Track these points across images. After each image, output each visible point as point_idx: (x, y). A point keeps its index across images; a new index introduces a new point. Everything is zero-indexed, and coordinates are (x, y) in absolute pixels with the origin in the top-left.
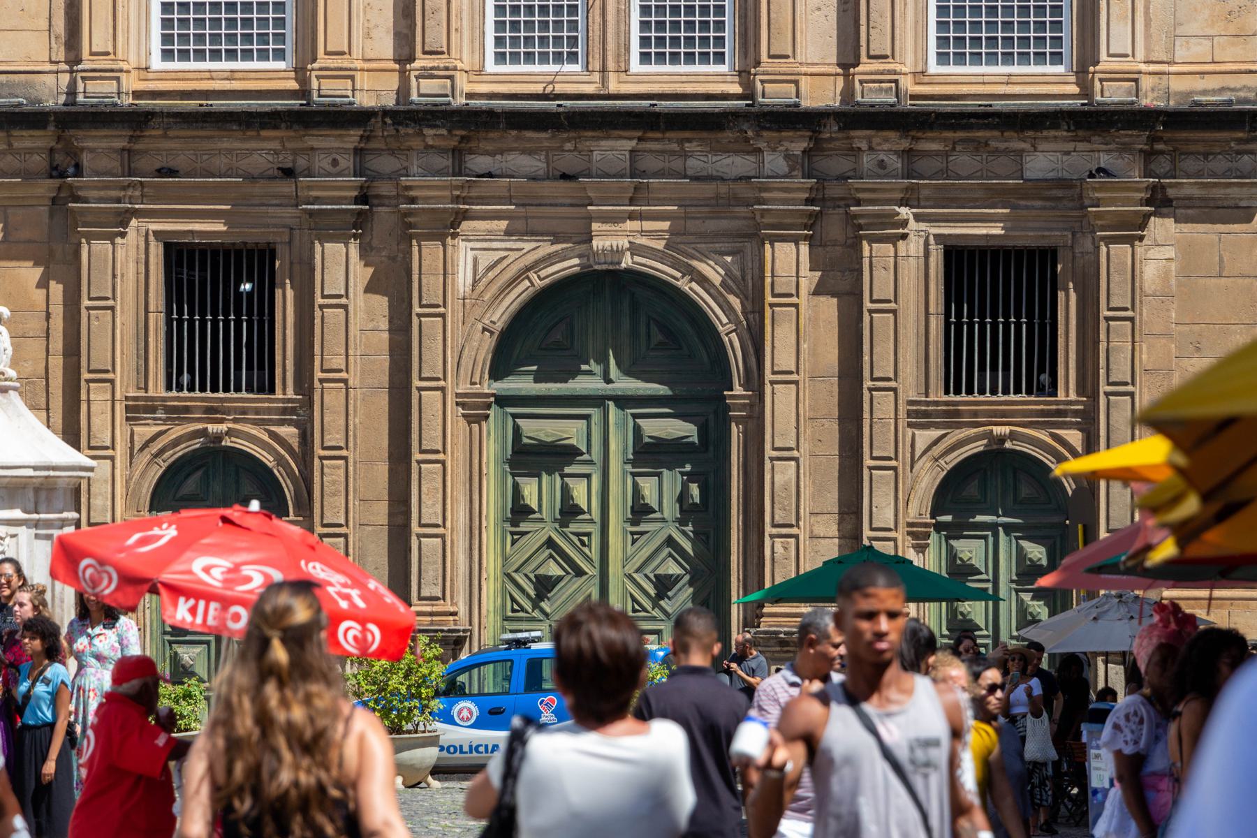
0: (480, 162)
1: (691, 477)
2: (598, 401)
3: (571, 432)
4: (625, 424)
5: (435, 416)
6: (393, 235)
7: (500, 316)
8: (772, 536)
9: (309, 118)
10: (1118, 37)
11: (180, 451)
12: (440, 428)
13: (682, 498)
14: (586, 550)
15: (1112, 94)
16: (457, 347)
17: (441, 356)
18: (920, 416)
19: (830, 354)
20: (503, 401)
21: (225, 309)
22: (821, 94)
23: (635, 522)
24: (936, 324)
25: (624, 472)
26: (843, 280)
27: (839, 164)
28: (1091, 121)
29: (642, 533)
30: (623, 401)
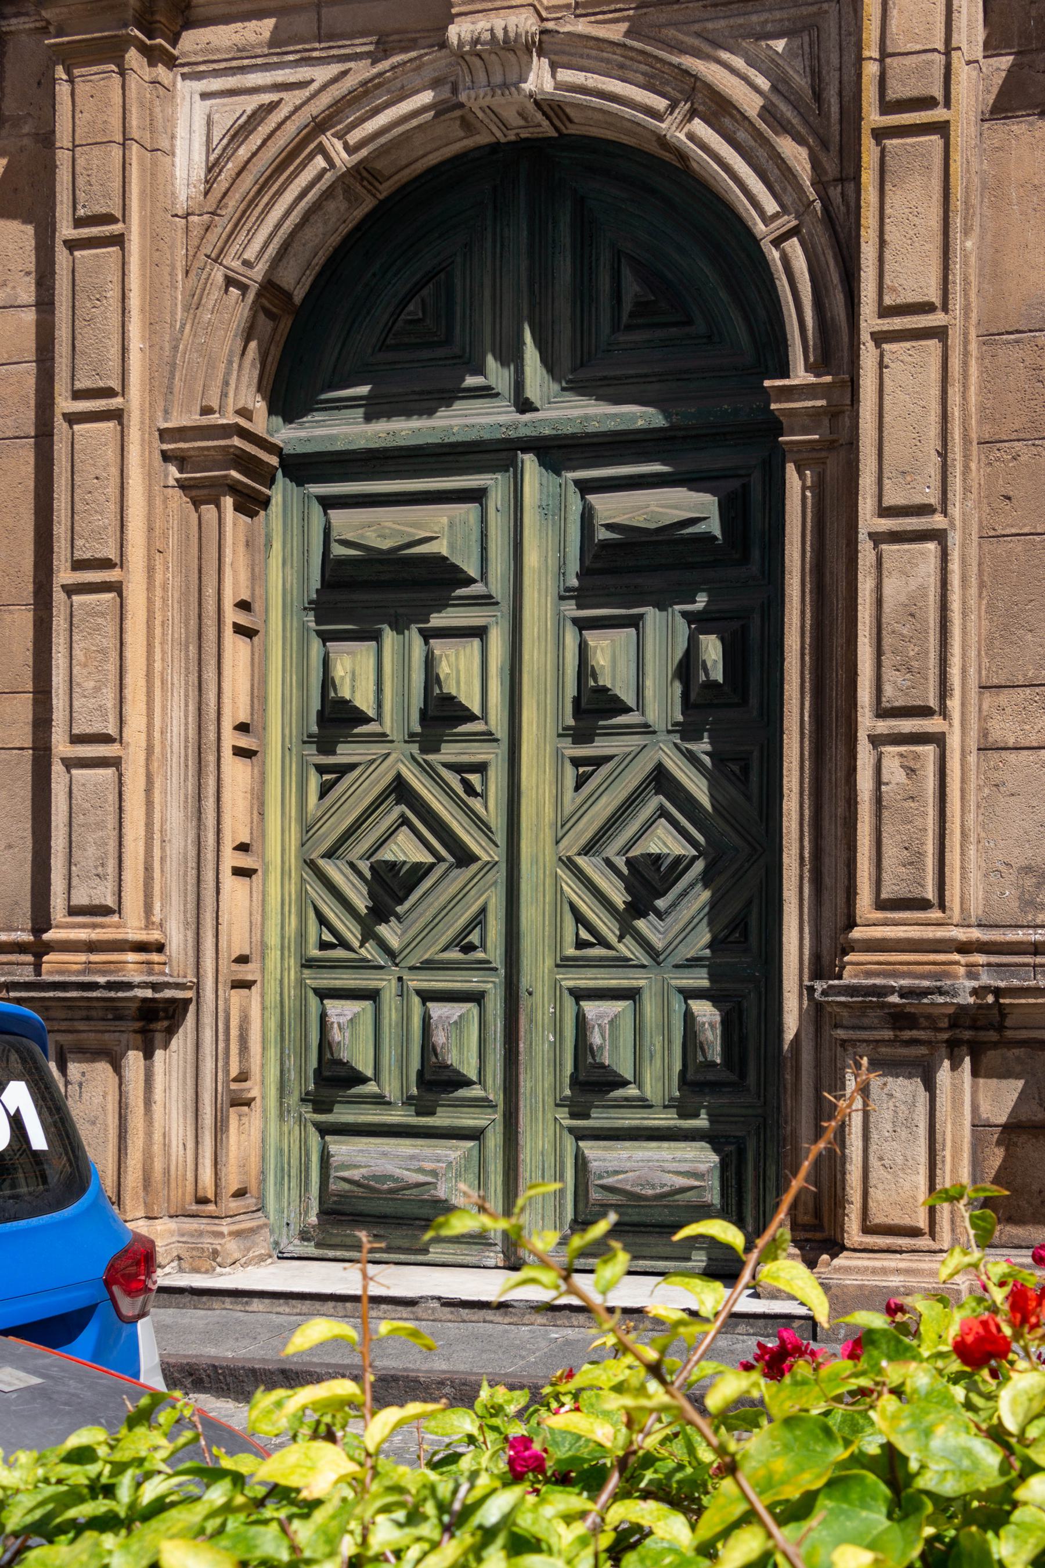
1: (700, 622)
2: (498, 453)
3: (440, 530)
4: (563, 507)
8: (876, 741)
12: (113, 507)
13: (687, 668)
14: (476, 804)
17: (116, 337)
20: (302, 468)
23: (581, 735)
25: (560, 621)
29: (598, 762)
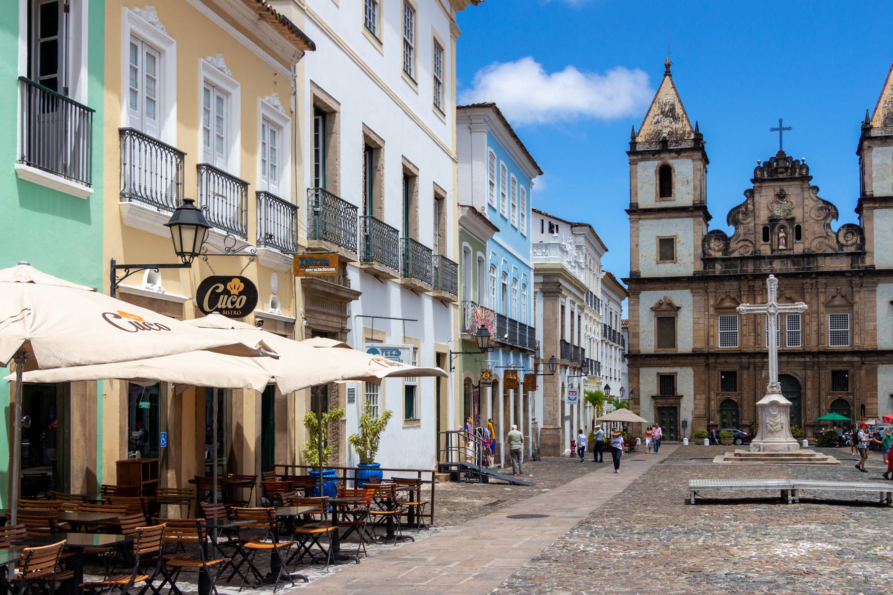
10: (857, 341)
15: (856, 349)
18: (829, 394)
21: (730, 380)
22: (815, 350)
28: (853, 353)
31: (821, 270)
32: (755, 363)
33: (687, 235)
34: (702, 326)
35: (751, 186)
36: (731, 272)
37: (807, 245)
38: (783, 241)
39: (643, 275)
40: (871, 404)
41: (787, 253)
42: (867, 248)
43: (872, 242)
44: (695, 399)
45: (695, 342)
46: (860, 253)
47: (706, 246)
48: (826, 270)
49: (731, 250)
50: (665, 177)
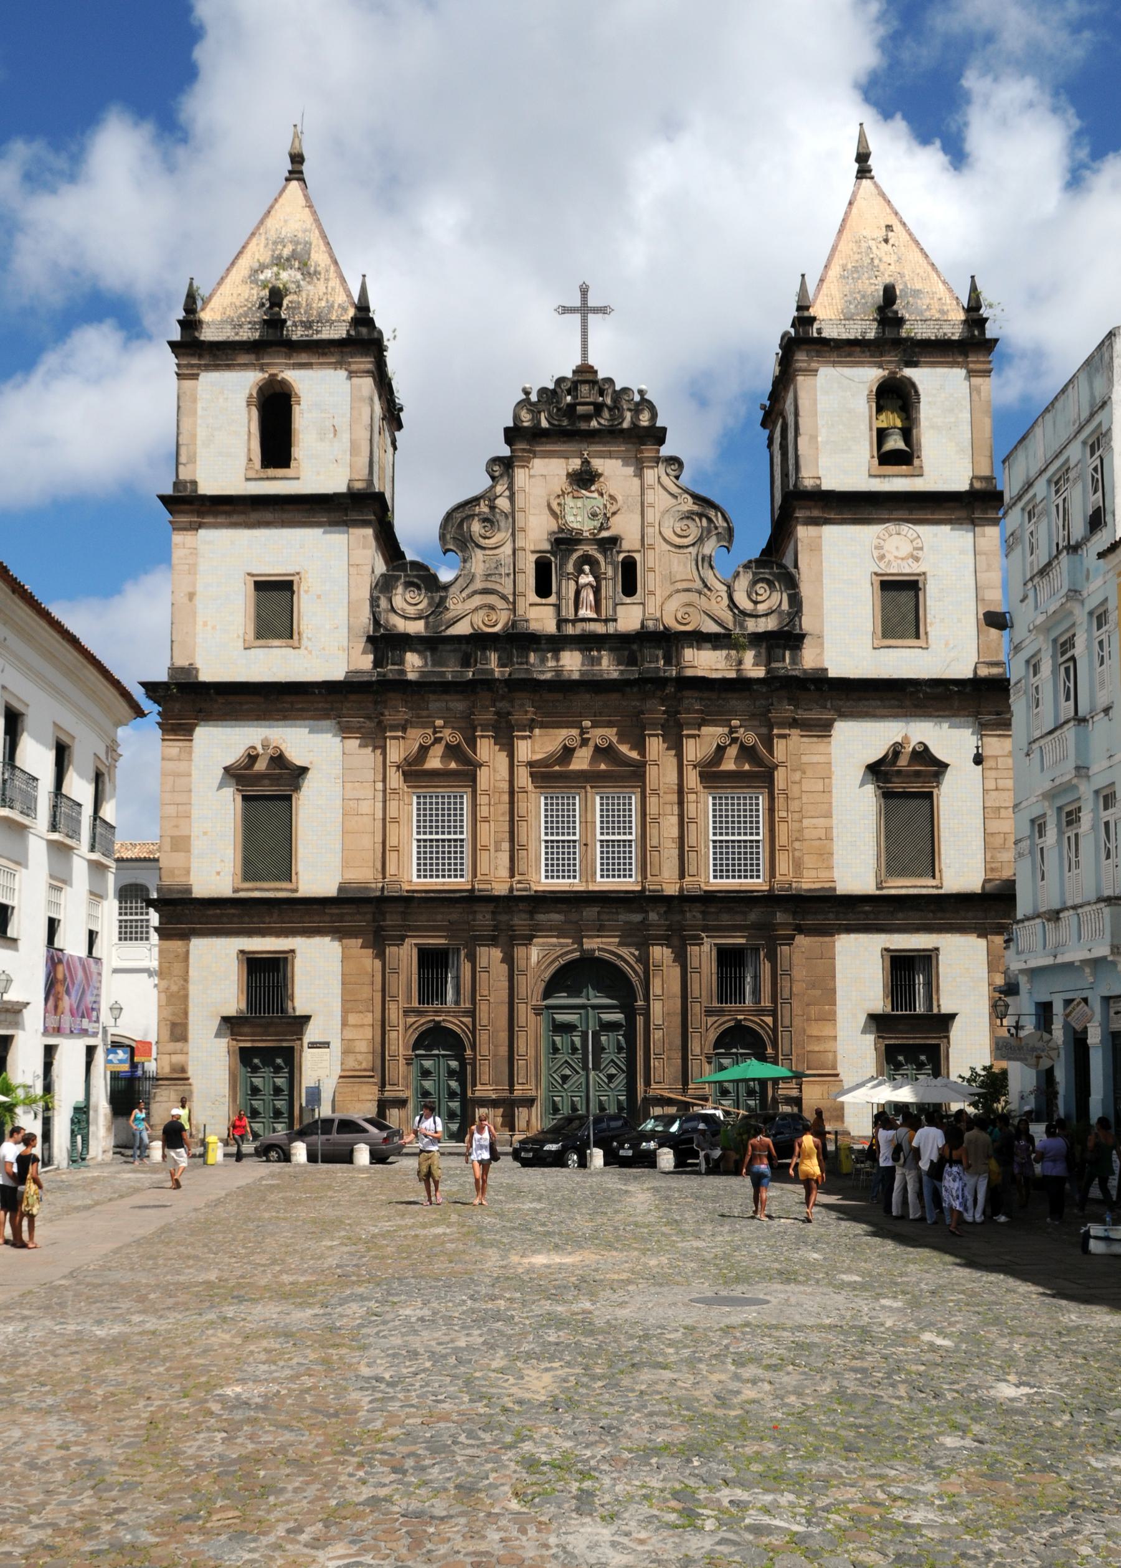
0: (541, 917)
5: (524, 1013)
6: (510, 941)
7: (547, 975)
9: (471, 900)
10: (783, 866)
11: (424, 1028)
16: (531, 986)
18: (709, 1012)
19: (676, 988)
22: (671, 890)
24: (714, 977)
26: (681, 958)
27: (677, 917)
28: (771, 900)
30: (594, 1007)
31: (689, 673)
32: (511, 928)
33: (331, 570)
34: (367, 820)
35: (505, 451)
36: (450, 671)
37: (652, 609)
38: (588, 596)
39: (205, 676)
40: (819, 1038)
41: (599, 628)
42: (807, 623)
43: (820, 607)
44: (344, 1024)
45: (346, 864)
46: (788, 638)
47: (383, 603)
48: (700, 674)
49: (449, 615)
50: (275, 416)
